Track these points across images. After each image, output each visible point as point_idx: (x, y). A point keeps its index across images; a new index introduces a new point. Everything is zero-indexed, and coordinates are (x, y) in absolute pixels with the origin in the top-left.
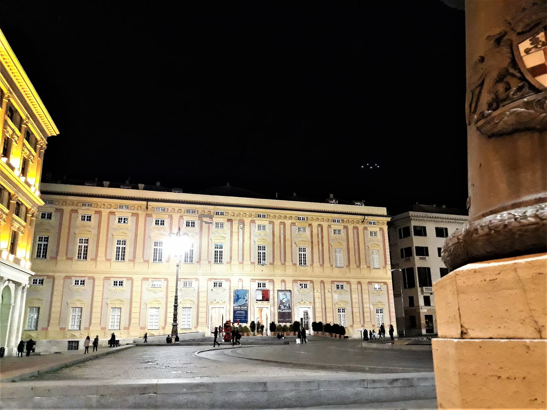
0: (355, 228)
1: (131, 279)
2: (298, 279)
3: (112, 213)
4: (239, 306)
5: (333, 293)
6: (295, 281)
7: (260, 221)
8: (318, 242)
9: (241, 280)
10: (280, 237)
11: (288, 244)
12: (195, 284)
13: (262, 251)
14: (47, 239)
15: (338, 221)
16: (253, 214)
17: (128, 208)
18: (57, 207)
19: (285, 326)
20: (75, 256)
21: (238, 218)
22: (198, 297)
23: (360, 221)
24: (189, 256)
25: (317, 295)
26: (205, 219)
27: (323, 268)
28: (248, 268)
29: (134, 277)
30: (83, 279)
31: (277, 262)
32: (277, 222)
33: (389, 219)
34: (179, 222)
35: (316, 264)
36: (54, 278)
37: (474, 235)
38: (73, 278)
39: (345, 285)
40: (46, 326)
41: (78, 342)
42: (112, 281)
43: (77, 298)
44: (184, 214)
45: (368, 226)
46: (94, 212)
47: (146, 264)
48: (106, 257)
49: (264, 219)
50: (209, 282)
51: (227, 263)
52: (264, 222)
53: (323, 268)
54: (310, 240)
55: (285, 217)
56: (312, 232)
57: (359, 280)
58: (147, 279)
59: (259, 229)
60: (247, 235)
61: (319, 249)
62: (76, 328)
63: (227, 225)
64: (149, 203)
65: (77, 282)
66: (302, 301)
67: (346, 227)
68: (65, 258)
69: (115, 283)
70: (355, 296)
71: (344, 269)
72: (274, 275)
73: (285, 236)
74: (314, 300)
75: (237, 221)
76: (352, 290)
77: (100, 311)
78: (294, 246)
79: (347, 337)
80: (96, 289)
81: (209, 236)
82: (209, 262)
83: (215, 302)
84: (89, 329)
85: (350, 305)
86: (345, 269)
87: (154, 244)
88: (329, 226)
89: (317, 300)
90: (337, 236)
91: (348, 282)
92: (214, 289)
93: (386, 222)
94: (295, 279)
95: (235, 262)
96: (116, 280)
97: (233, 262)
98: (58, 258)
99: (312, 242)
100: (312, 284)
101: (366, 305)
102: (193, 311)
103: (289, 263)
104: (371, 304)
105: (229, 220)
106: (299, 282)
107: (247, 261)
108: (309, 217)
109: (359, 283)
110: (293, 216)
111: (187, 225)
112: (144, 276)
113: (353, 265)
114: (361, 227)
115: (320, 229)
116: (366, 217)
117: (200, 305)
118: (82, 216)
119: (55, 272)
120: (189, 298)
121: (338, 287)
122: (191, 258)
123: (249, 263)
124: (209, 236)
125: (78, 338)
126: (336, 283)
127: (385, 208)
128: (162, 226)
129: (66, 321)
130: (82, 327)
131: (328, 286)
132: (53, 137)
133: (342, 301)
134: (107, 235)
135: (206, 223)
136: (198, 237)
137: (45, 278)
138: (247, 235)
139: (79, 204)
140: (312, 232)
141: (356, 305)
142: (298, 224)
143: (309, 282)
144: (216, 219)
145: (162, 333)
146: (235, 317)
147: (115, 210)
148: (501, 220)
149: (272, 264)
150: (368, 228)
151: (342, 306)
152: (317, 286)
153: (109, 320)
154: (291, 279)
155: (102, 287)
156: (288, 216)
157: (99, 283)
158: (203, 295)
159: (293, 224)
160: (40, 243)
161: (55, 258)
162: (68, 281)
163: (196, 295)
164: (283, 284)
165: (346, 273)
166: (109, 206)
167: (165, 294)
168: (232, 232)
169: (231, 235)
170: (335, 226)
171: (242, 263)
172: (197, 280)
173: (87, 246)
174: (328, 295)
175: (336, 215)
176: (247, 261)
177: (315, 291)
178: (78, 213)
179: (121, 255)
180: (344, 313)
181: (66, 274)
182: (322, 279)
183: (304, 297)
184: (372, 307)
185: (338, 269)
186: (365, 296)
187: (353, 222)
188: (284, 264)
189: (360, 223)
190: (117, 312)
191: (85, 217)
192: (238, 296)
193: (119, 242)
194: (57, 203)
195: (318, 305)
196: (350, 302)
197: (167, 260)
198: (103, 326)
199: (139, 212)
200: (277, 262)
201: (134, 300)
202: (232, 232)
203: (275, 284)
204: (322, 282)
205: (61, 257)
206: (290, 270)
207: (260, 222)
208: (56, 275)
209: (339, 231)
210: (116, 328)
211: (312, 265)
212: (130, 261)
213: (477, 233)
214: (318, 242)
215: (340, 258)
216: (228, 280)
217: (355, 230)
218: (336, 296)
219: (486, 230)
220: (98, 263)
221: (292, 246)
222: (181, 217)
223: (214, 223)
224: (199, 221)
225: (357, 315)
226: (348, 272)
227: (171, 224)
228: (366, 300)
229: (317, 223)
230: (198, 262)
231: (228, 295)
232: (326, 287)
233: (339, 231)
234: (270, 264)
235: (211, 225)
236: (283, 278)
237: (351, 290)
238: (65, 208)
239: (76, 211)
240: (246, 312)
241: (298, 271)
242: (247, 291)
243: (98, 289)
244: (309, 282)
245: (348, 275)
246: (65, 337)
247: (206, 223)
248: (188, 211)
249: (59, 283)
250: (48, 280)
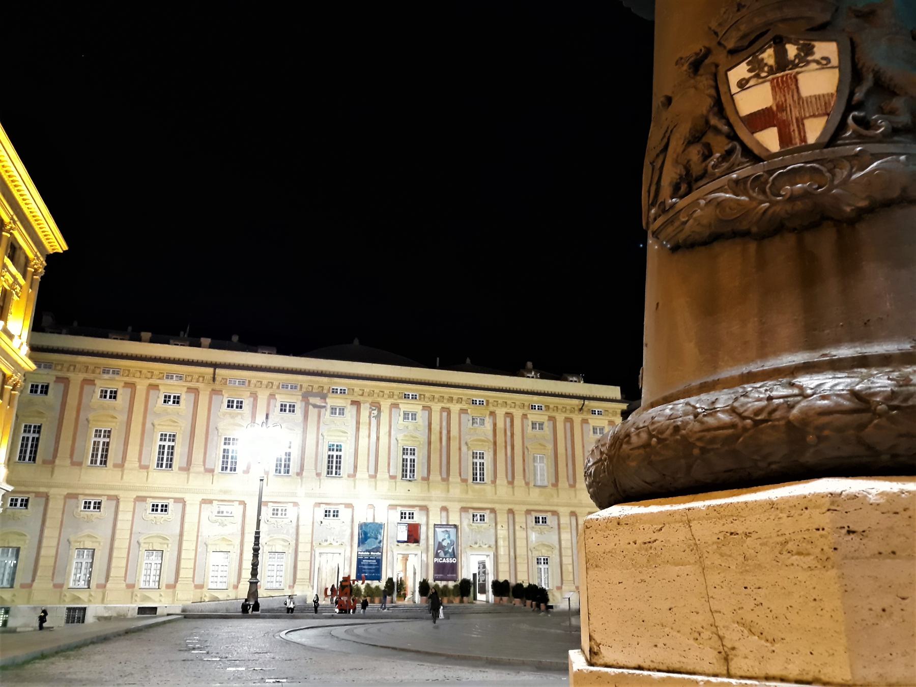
0: (569, 420)
1: (182, 501)
2: (469, 505)
3: (155, 387)
4: (367, 551)
6: (464, 509)
7: (406, 406)
8: (506, 442)
9: (372, 506)
10: (441, 433)
11: (454, 445)
12: (292, 513)
13: (409, 457)
14: (38, 429)
15: (540, 408)
16: (396, 392)
17: (181, 378)
18: (60, 374)
19: (446, 587)
20: (87, 458)
21: (370, 400)
22: (297, 534)
23: (576, 408)
24: (283, 463)
25: (502, 532)
26: (312, 400)
27: (513, 488)
28: (384, 485)
29: (187, 497)
30: (98, 500)
31: (435, 477)
32: (436, 407)
33: (624, 406)
34: (268, 405)
35: (502, 480)
36: (47, 497)
37: (624, 446)
38: (81, 497)
39: (549, 517)
40: (29, 581)
41: (85, 609)
42: (150, 502)
43: (87, 532)
44: (277, 391)
45: (590, 417)
46: (122, 384)
47: (209, 476)
48: (140, 460)
49: (413, 401)
50: (316, 509)
51: (349, 476)
52: (415, 407)
53: (513, 488)
54: (491, 438)
55: (451, 399)
56: (495, 425)
58: (210, 502)
59: (404, 418)
60: (384, 429)
61: (506, 454)
62: (82, 584)
63: (351, 411)
64: (218, 370)
65: (87, 505)
66: (476, 543)
67: (552, 419)
68: (68, 461)
69: (155, 508)
71: (547, 490)
73: (449, 432)
74: (496, 542)
75: (368, 405)
76: (561, 526)
77: (125, 556)
78: (464, 448)
79: (551, 607)
80: (120, 517)
81: (318, 428)
82: (318, 475)
83: (326, 544)
84: (105, 586)
85: (556, 552)
86: (550, 490)
87: (223, 441)
88: (525, 416)
89: (501, 543)
90: (537, 431)
91: (555, 513)
93: (619, 411)
94: (464, 505)
95: (362, 473)
96: (156, 502)
97: (358, 475)
98: (57, 462)
99: (495, 443)
100: (492, 515)
102: (288, 560)
103: (454, 478)
105: (354, 403)
106: (471, 511)
107: (383, 474)
108: (491, 400)
109: (573, 514)
110: (464, 398)
111: (281, 410)
112: (205, 497)
113: (563, 483)
114: (577, 418)
115: (508, 420)
116: (587, 402)
117: (300, 549)
118: (102, 391)
119: (51, 487)
120: (282, 536)
121: (537, 520)
122: (287, 466)
123: (387, 476)
124: (318, 428)
125: (84, 602)
126: (534, 514)
127: (618, 388)
128: (239, 410)
129: (65, 573)
130: (93, 584)
131: (520, 519)
132: (57, 254)
133: (544, 545)
134: (144, 424)
135: (315, 406)
136: (299, 431)
137: (32, 497)
138: (384, 429)
139: (98, 371)
140: (495, 425)
142: (471, 409)
143: (488, 511)
144: (332, 401)
145: (232, 596)
146: (359, 570)
147: (158, 382)
148: (670, 418)
149: (426, 479)
150: (590, 421)
151: (544, 553)
152: (502, 518)
153: (141, 572)
154: (458, 506)
155: (131, 514)
156: (455, 397)
157: (126, 507)
158: (305, 531)
159: (463, 411)
160: (26, 435)
161: (51, 462)
162: (71, 502)
163: (293, 531)
164: (444, 514)
165: (552, 496)
166: (149, 375)
167: (240, 528)
168: (358, 423)
169: (358, 429)
170: (534, 416)
171: (375, 476)
172: (296, 504)
173: (108, 443)
174: (520, 534)
175: (536, 398)
176: (383, 474)
177: (499, 527)
178: (95, 385)
179: (166, 459)
180: (546, 566)
181: (70, 491)
182: (510, 507)
183: (479, 536)
185: (537, 490)
187: (564, 410)
188: (446, 480)
189: (577, 412)
190: (155, 559)
191: (106, 392)
192: (365, 533)
193: (163, 437)
194: (59, 367)
195: (502, 551)
196: (557, 546)
197: (245, 469)
198: (130, 581)
199: (200, 385)
200: (435, 477)
201: (185, 538)
202: (358, 423)
203: (431, 514)
204: (511, 511)
205: (62, 461)
206: (456, 490)
207: (405, 406)
208: (52, 491)
209: (541, 424)
210: (152, 585)
211: (494, 482)
212: (181, 469)
213: (629, 443)
214: (506, 442)
215: (542, 470)
216: (349, 506)
217: (568, 425)
218: (533, 536)
219: (644, 436)
220: (125, 472)
221: (460, 449)
222: (272, 396)
223: (329, 407)
224: (304, 404)
226: (555, 496)
227: (254, 406)
229: (504, 410)
230: (299, 474)
231: (349, 531)
232: (517, 520)
233: (541, 424)
234: (423, 479)
235: (323, 410)
236: (444, 504)
237: (559, 525)
238: (71, 375)
239: (91, 382)
240: (379, 562)
241: (470, 492)
242: (380, 526)
243: (125, 517)
244: (488, 511)
245: (555, 500)
246: (61, 600)
247: (315, 406)
248: (285, 386)
249: (55, 506)
250: (38, 499)
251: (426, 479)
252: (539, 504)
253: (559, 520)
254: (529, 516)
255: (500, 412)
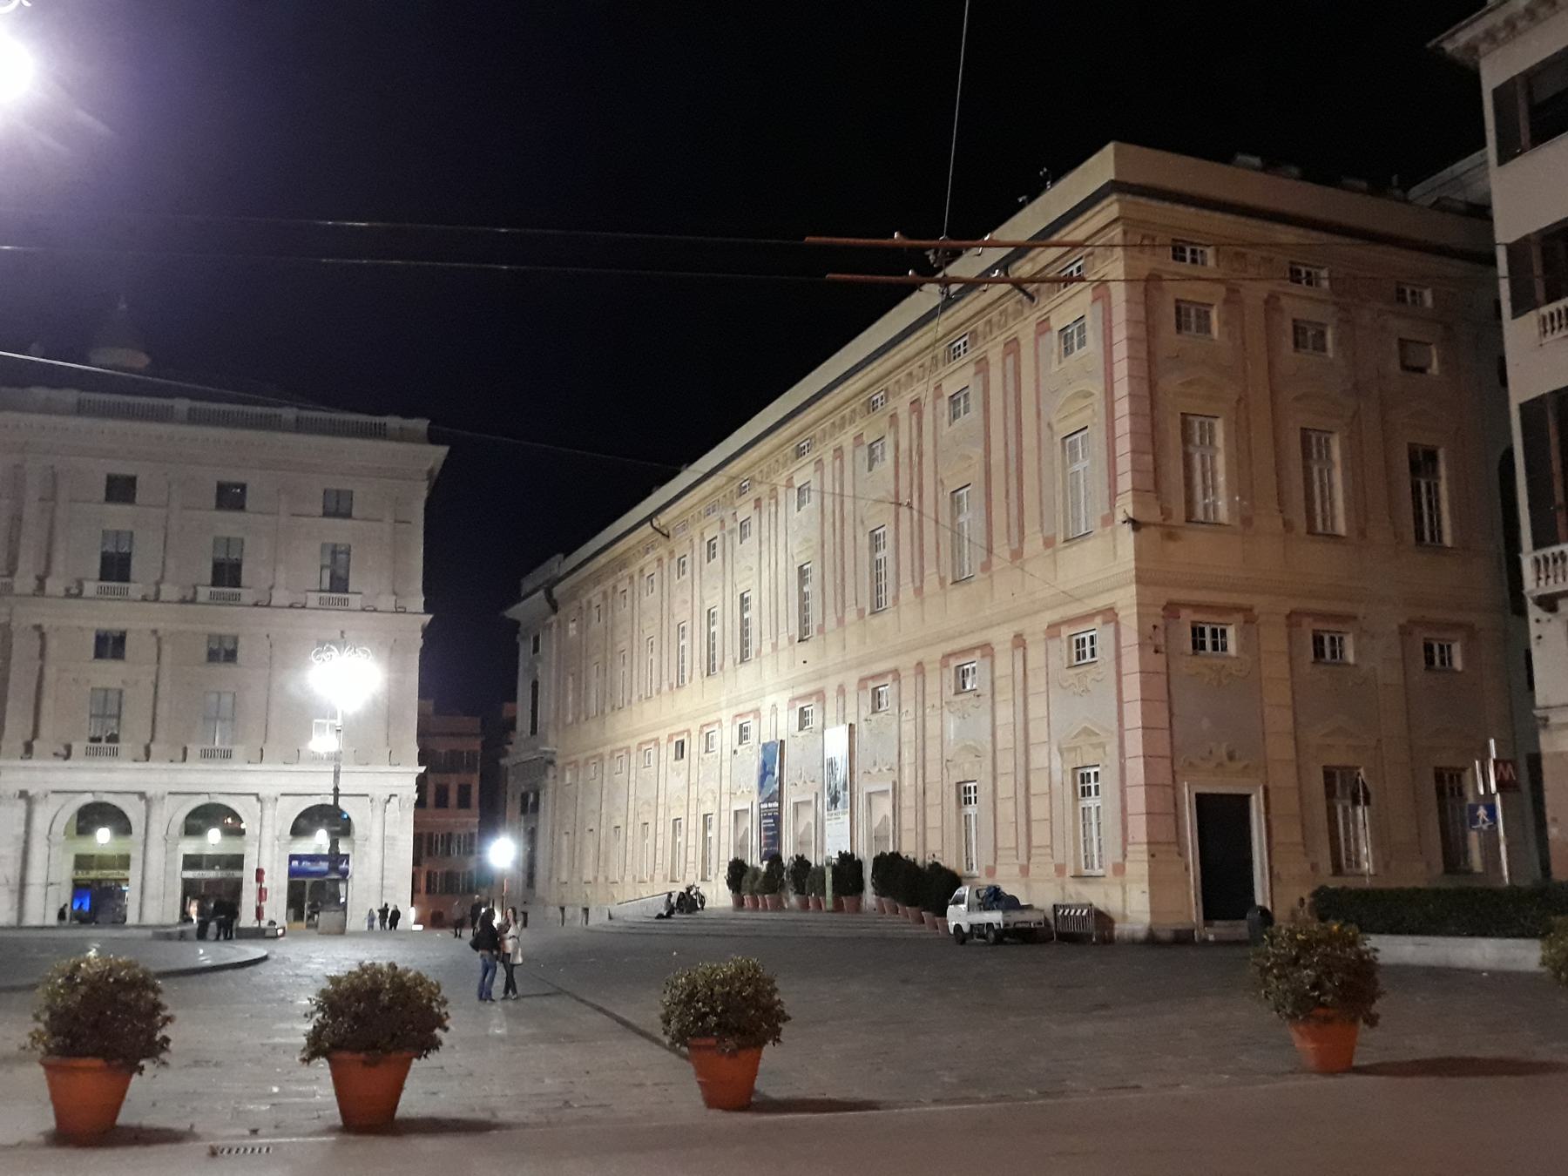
2: (866, 673)
5: (946, 710)
25: (908, 728)
27: (922, 602)
52: (804, 473)
57: (1016, 627)
70: (1005, 714)
72: (821, 676)
85: (988, 763)
92: (739, 749)
101: (1039, 758)
103: (851, 615)
104: (1055, 749)
114: (1025, 329)
133: (966, 747)
141: (1006, 763)
149: (821, 630)
159: (858, 438)
184: (1057, 763)
186: (1037, 708)
196: (989, 747)
225: (1006, 810)
228: (1038, 732)
251: (821, 630)
252: (961, 634)
253: (993, 672)
254: (945, 671)
255: (902, 405)
